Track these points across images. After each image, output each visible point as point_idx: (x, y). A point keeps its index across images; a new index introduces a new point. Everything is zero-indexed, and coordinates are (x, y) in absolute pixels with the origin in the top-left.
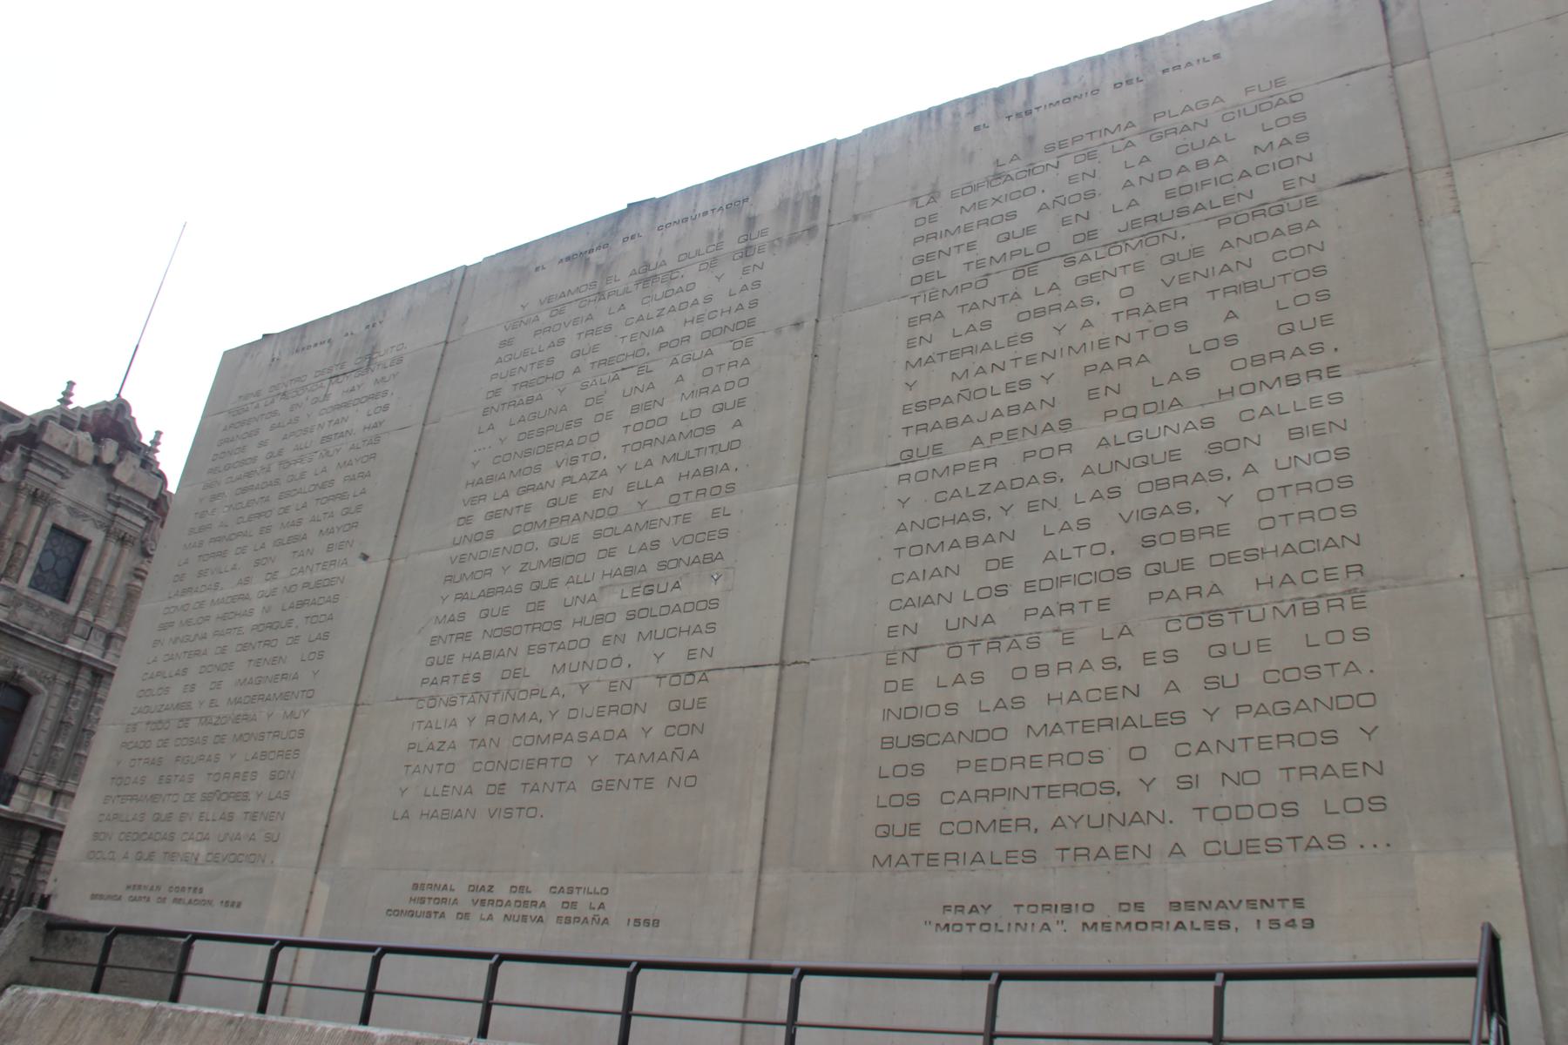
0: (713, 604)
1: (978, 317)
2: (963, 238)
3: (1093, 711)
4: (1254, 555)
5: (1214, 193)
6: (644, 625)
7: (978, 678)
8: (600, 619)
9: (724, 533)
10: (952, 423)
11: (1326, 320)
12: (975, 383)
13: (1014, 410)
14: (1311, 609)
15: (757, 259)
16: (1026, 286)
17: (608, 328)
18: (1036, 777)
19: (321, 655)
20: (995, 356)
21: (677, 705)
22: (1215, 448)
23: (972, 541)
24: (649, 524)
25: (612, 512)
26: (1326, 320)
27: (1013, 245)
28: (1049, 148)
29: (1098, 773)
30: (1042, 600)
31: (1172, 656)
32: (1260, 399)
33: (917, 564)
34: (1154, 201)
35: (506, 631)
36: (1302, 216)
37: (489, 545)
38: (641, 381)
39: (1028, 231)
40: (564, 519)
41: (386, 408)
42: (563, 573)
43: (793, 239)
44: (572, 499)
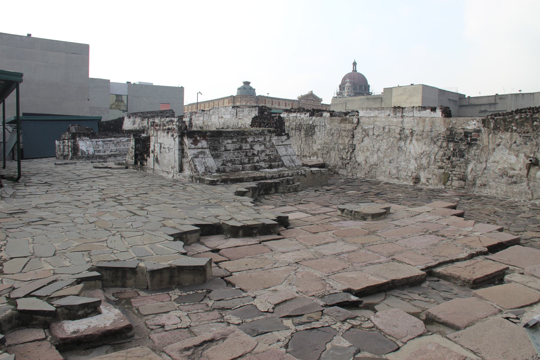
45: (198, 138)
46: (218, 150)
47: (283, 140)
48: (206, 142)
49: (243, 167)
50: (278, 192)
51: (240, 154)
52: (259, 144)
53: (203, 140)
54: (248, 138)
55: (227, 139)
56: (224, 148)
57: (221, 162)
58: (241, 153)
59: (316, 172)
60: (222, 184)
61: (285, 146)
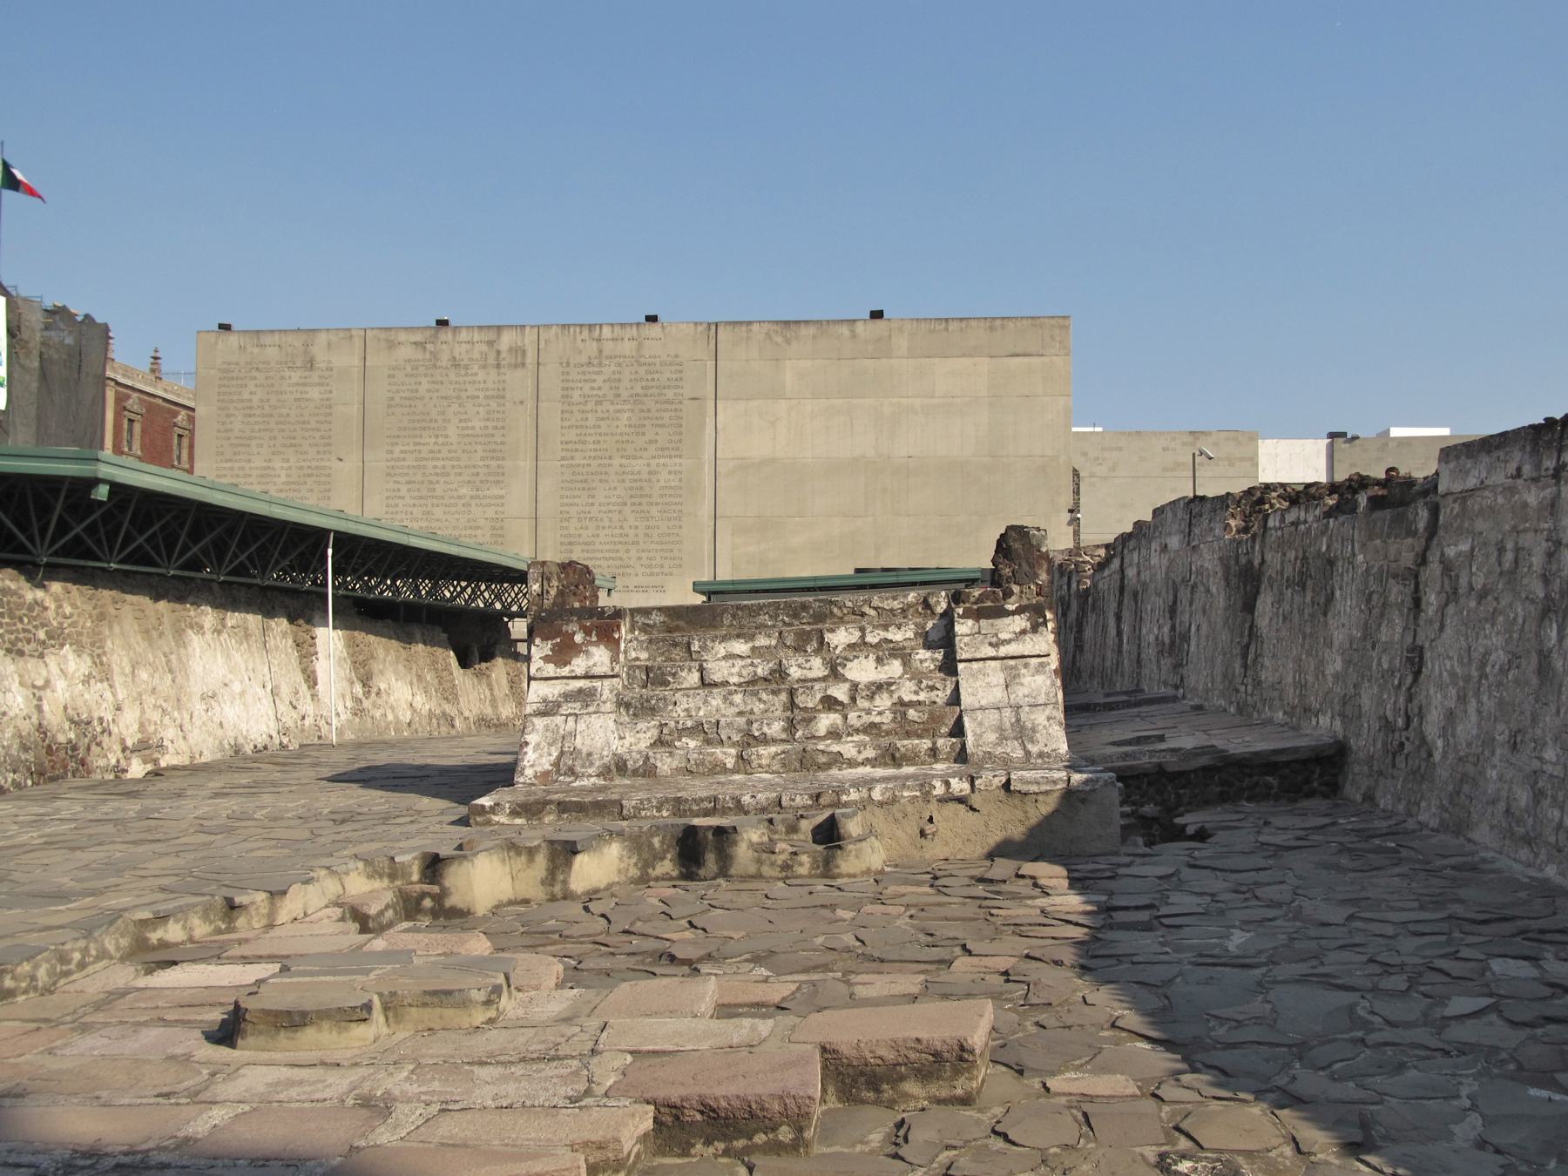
0: (502, 497)
1: (584, 416)
2: (580, 385)
3: (617, 539)
4: (657, 504)
5: (654, 391)
6: (478, 501)
7: (587, 528)
8: (460, 497)
9: (503, 474)
10: (577, 450)
11: (680, 441)
12: (583, 438)
13: (595, 450)
14: (670, 519)
15: (503, 370)
16: (599, 408)
17: (442, 383)
18: (601, 555)
19: (329, 498)
20: (589, 431)
21: (494, 528)
22: (650, 473)
23: (584, 489)
24: (474, 467)
25: (458, 459)
26: (680, 441)
27: (595, 392)
28: (607, 357)
29: (618, 555)
30: (604, 509)
31: (636, 527)
32: (662, 461)
33: (568, 493)
34: (638, 390)
35: (421, 498)
36: (678, 407)
37: (406, 463)
38: (461, 409)
39: (600, 388)
40: (438, 459)
41: (331, 392)
42: (442, 480)
43: (516, 366)
44: (439, 451)
45: (578, 638)
46: (666, 683)
47: (1003, 636)
48: (611, 651)
49: (740, 757)
50: (732, 871)
51: (760, 700)
52: (872, 657)
53: (596, 644)
54: (832, 631)
55: (724, 639)
56: (696, 676)
57: (649, 734)
58: (764, 696)
59: (1034, 788)
60: (519, 821)
61: (1012, 662)
